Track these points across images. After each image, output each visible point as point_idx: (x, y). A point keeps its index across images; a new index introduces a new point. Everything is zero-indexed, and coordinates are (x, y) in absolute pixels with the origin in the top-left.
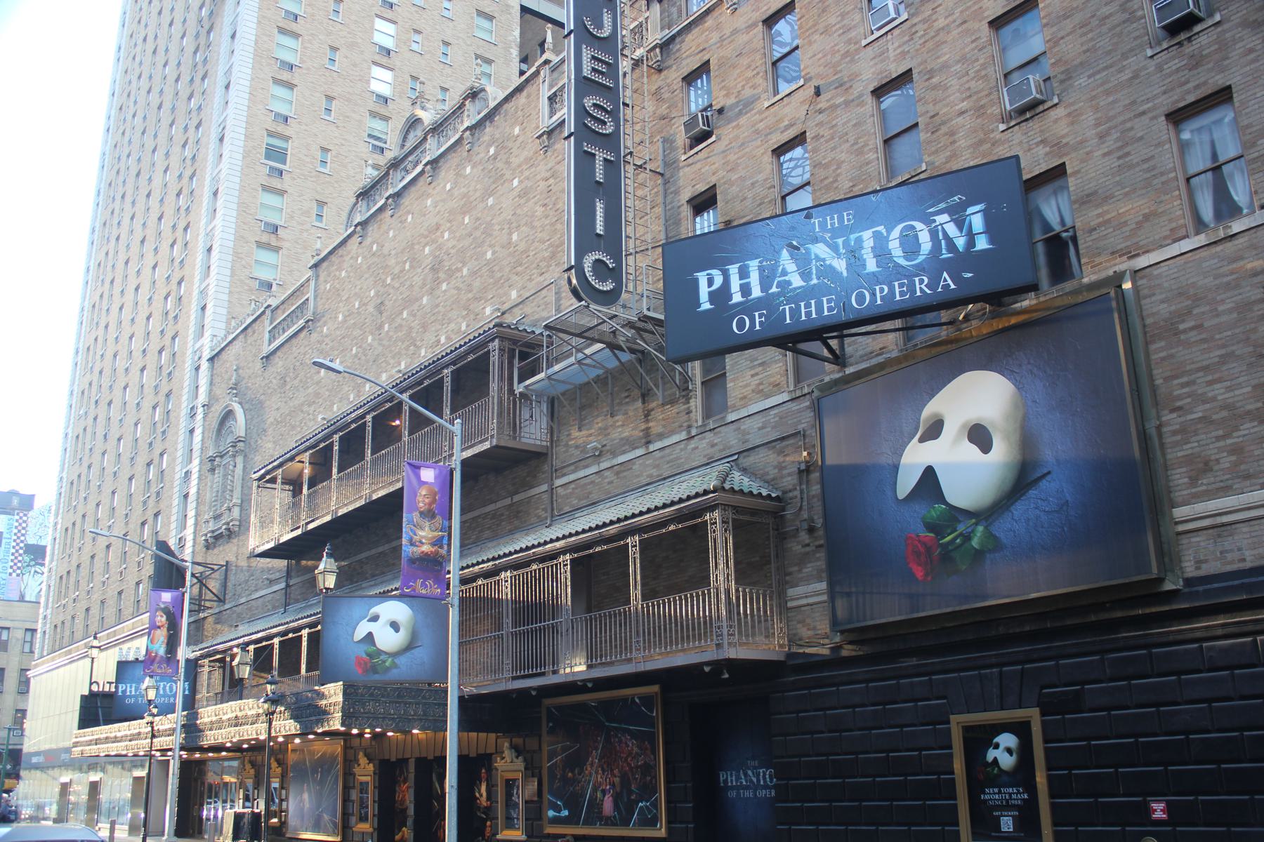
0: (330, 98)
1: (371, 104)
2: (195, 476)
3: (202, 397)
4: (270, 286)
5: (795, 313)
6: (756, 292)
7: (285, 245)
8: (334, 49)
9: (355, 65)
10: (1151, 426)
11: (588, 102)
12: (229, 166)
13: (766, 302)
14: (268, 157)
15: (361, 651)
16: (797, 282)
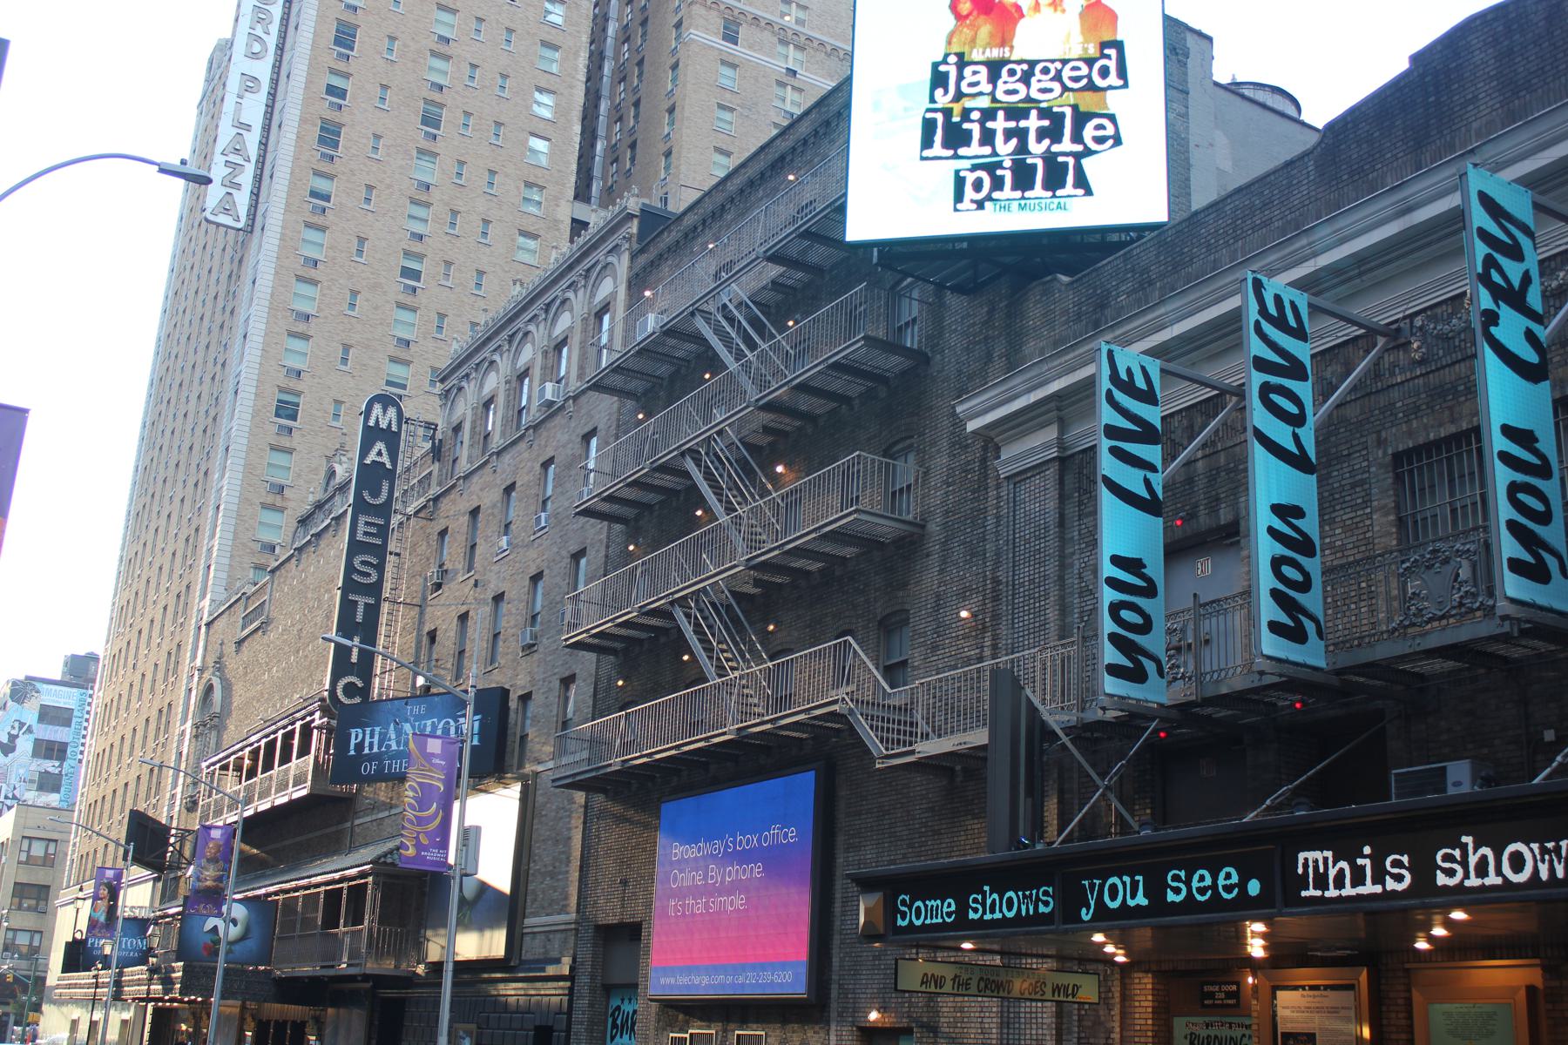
0: (346, 348)
1: (392, 350)
2: (188, 737)
3: (198, 662)
4: (273, 548)
5: (390, 766)
6: (375, 749)
7: (291, 504)
8: (354, 293)
9: (376, 308)
10: (524, 867)
11: (357, 562)
12: (242, 419)
13: (378, 757)
14: (277, 415)
15: (208, 939)
16: (394, 747)
